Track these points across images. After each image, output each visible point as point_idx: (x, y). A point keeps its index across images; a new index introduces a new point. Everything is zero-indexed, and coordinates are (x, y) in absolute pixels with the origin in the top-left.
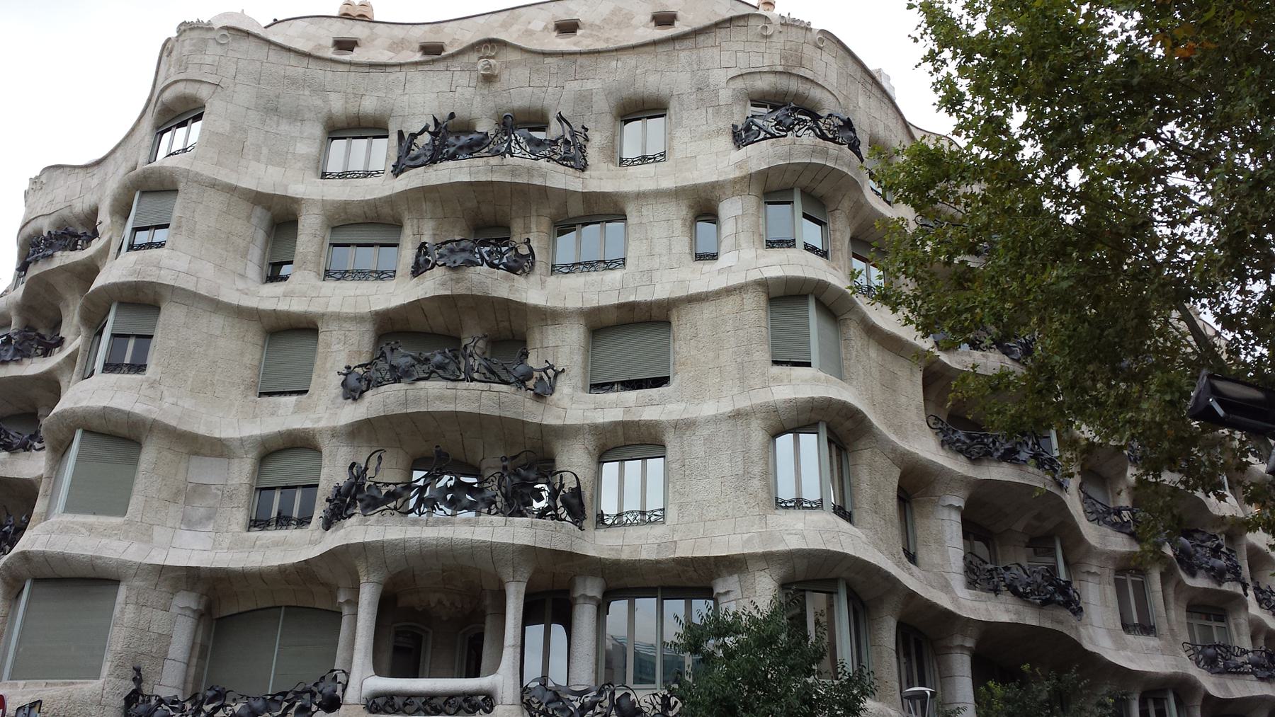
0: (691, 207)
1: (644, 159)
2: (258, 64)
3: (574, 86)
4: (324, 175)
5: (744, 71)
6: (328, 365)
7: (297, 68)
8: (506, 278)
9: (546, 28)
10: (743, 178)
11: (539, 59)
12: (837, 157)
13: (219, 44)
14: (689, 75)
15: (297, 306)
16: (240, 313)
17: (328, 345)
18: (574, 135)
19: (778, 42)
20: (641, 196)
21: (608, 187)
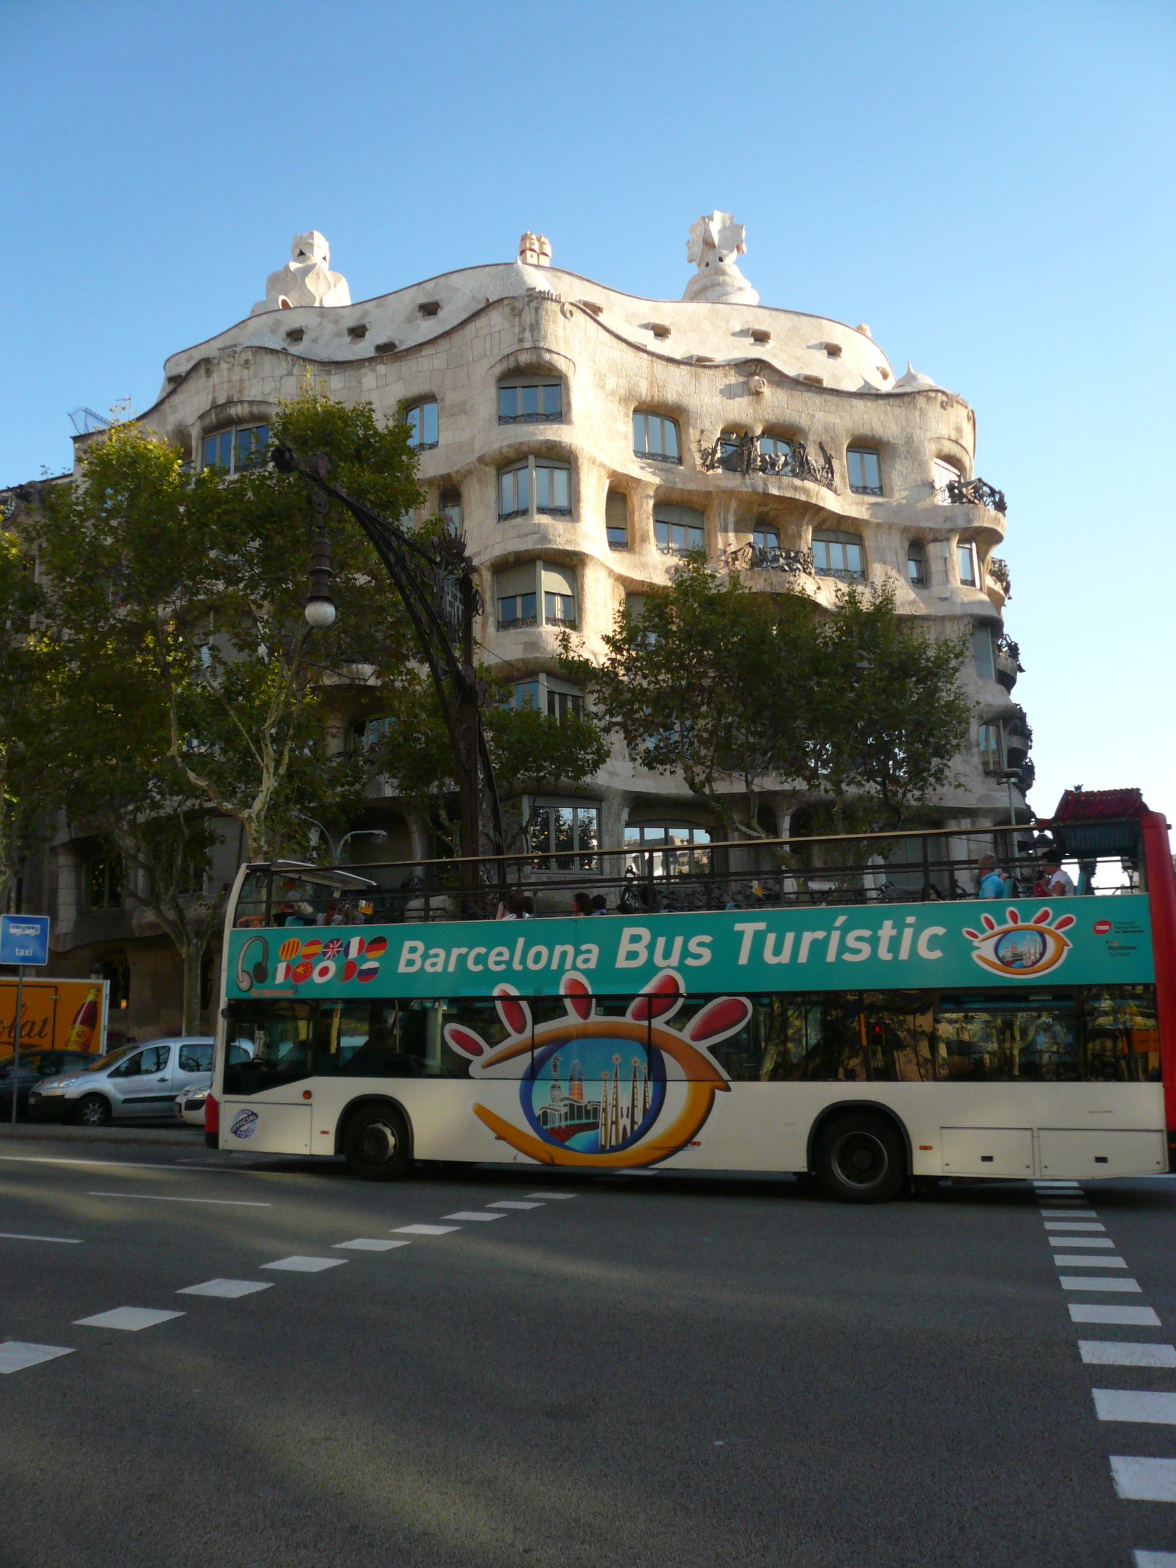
13: (565, 317)
16: (622, 580)
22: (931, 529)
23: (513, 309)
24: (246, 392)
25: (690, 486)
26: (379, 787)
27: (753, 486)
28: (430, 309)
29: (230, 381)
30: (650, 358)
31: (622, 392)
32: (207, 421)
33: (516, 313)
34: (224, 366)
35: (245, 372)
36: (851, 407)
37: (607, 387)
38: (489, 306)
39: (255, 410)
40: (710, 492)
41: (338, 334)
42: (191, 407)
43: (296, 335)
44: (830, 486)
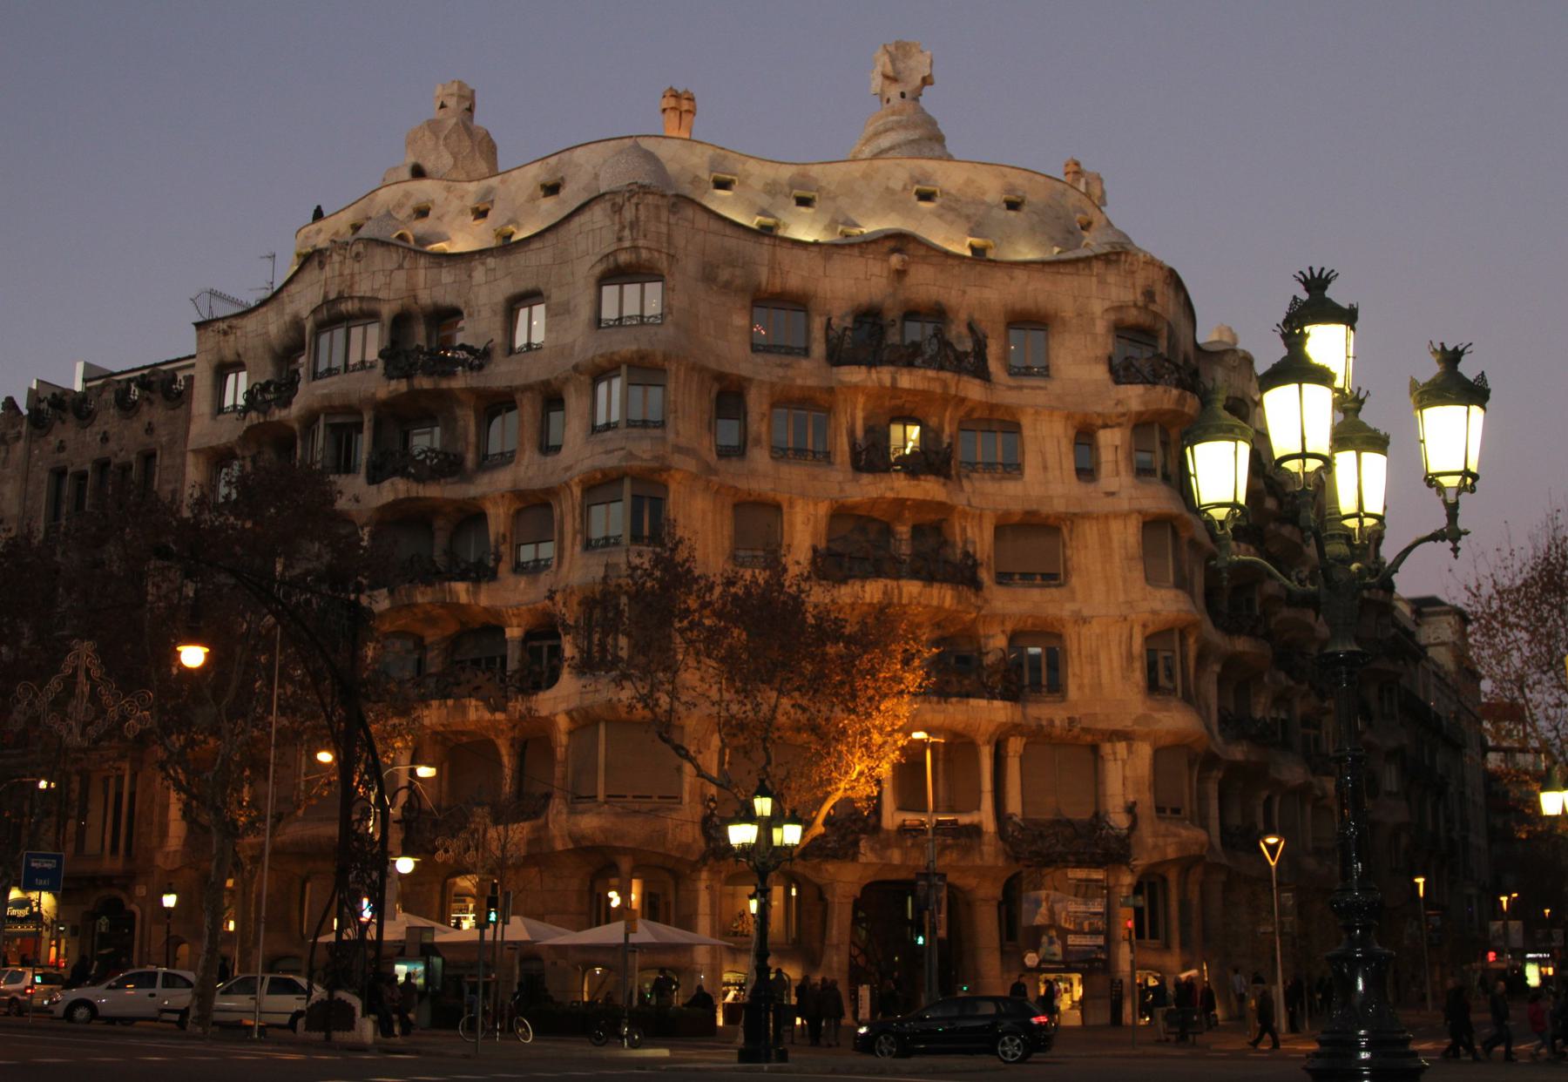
3: (973, 294)
4: (755, 348)
9: (905, 188)
10: (1124, 415)
17: (792, 525)
19: (1140, 280)
22: (1099, 415)
23: (614, 205)
24: (356, 287)
26: (464, 710)
28: (552, 189)
29: (341, 275)
31: (739, 282)
32: (320, 317)
33: (617, 209)
34: (336, 258)
35: (357, 266)
36: (1012, 278)
38: (599, 197)
39: (365, 306)
41: (462, 212)
42: (305, 300)
43: (422, 213)
44: (982, 373)
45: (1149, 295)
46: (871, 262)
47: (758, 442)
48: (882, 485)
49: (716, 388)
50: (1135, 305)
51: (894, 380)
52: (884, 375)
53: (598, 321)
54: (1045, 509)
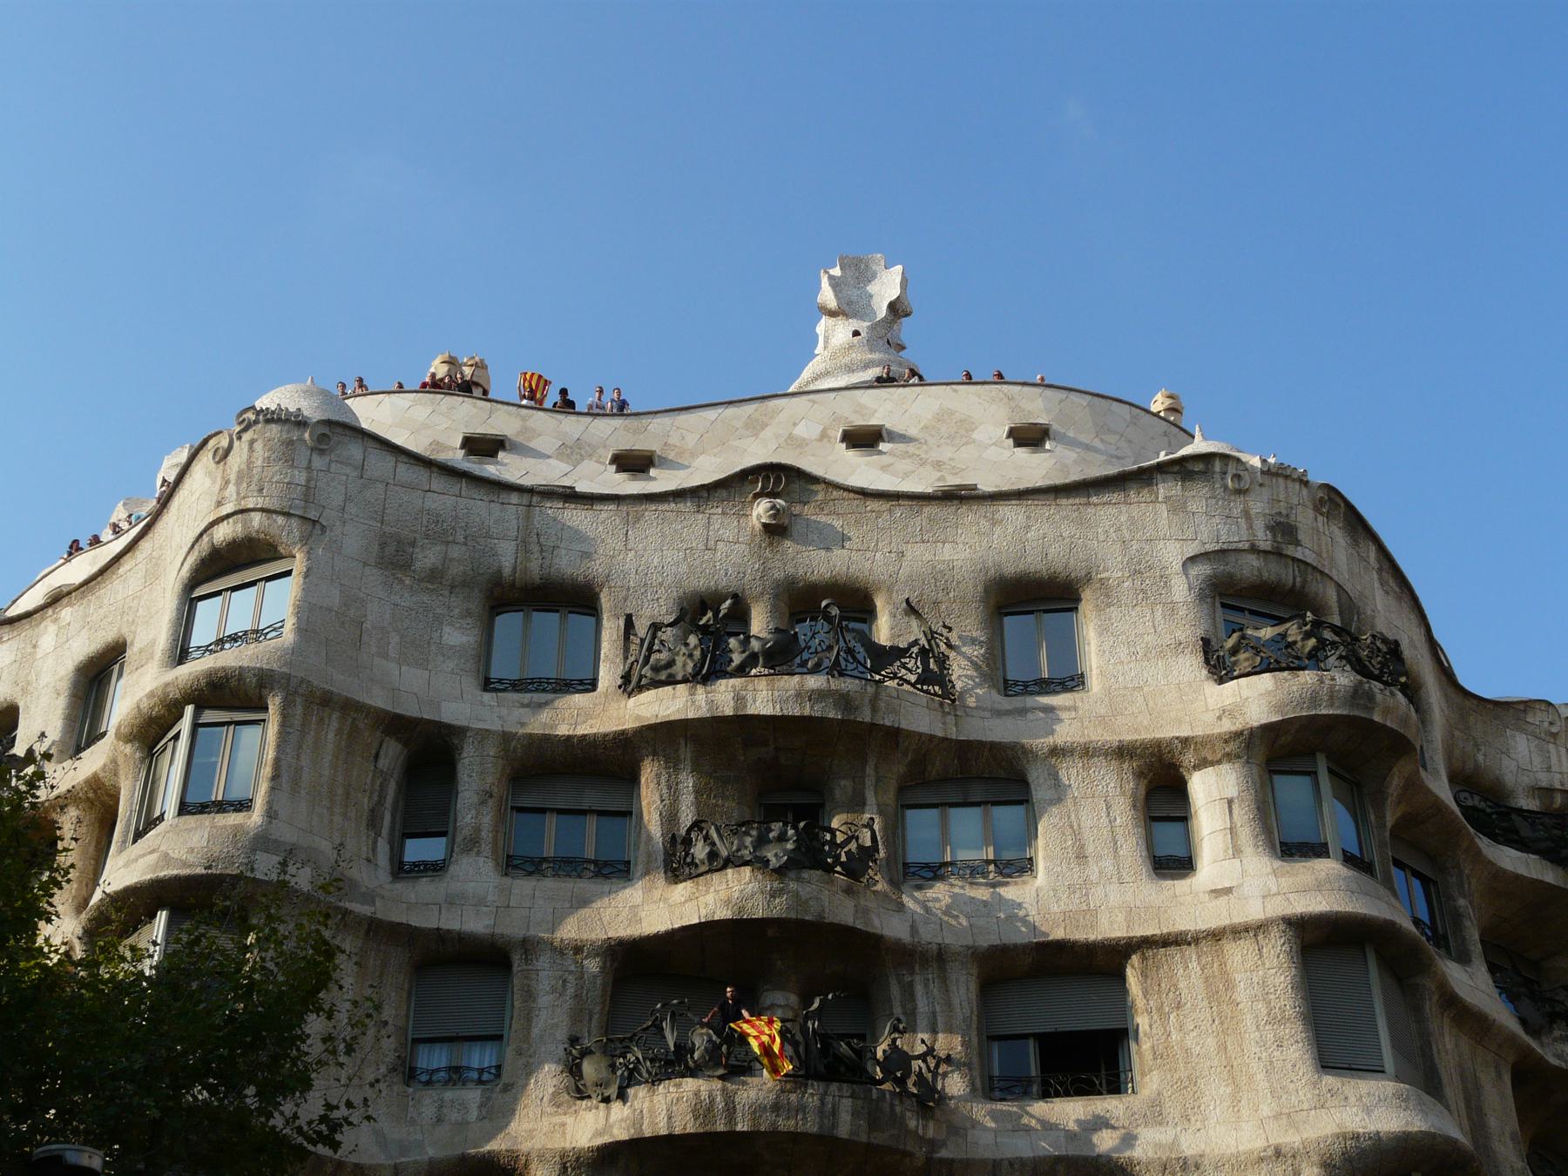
0: (1139, 775)
1: (1047, 686)
2: (381, 486)
4: (487, 685)
5: (1210, 547)
6: (535, 1031)
7: (444, 499)
8: (849, 891)
9: (824, 435)
11: (857, 502)
12: (1389, 707)
14: (1117, 547)
15: (475, 923)
17: (530, 995)
18: (931, 635)
19: (1258, 505)
20: (1055, 752)
21: (999, 731)
22: (1185, 741)
25: (582, 730)
27: (711, 703)
30: (525, 499)
31: (455, 570)
37: (418, 565)
40: (623, 732)
45: (1284, 529)
46: (717, 521)
47: (472, 844)
48: (710, 898)
49: (393, 753)
50: (1254, 549)
51: (739, 699)
52: (722, 697)
53: (181, 654)
54: (1079, 935)
